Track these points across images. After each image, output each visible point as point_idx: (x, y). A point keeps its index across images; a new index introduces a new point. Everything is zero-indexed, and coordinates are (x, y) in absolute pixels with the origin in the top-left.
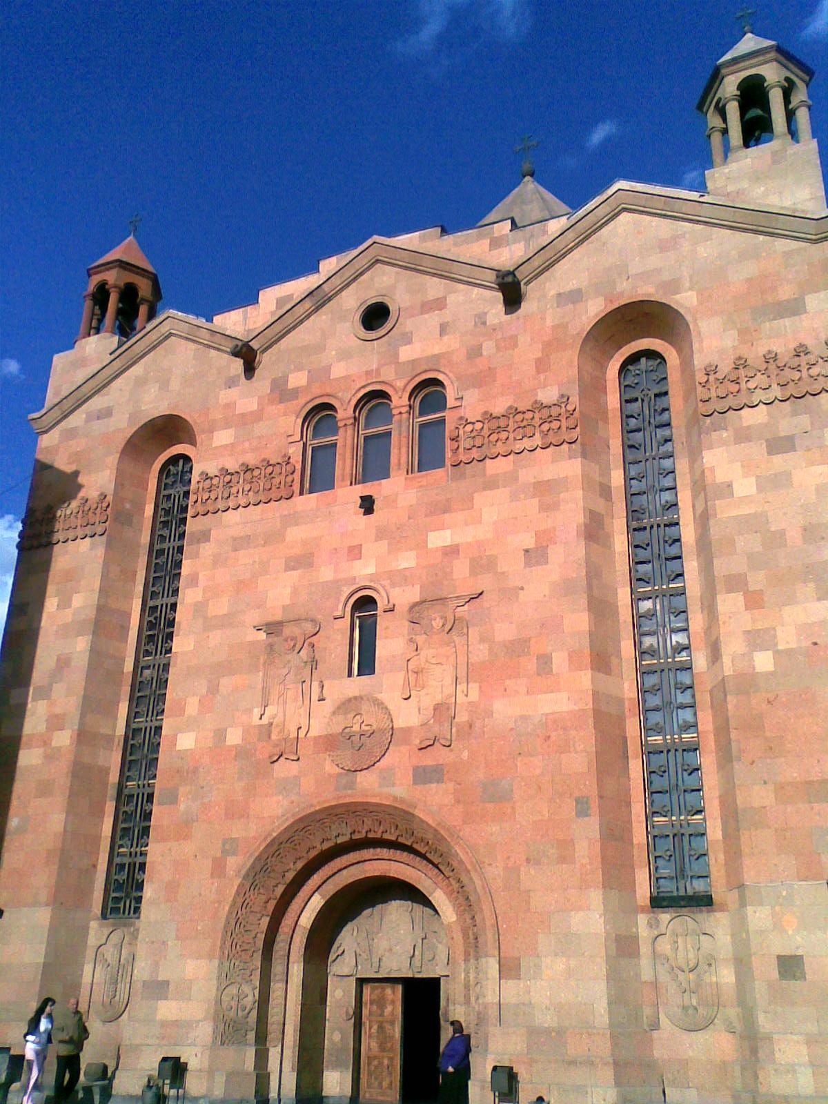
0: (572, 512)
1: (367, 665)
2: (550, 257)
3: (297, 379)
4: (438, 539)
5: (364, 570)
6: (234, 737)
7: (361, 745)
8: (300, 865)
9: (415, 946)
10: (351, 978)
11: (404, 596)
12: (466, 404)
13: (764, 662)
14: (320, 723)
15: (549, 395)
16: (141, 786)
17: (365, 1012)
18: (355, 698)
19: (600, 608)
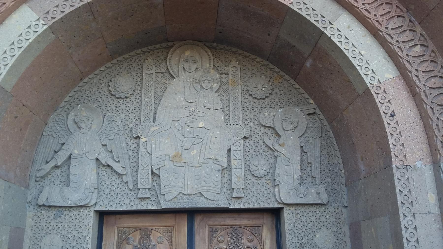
9: (229, 150)
10: (84, 212)
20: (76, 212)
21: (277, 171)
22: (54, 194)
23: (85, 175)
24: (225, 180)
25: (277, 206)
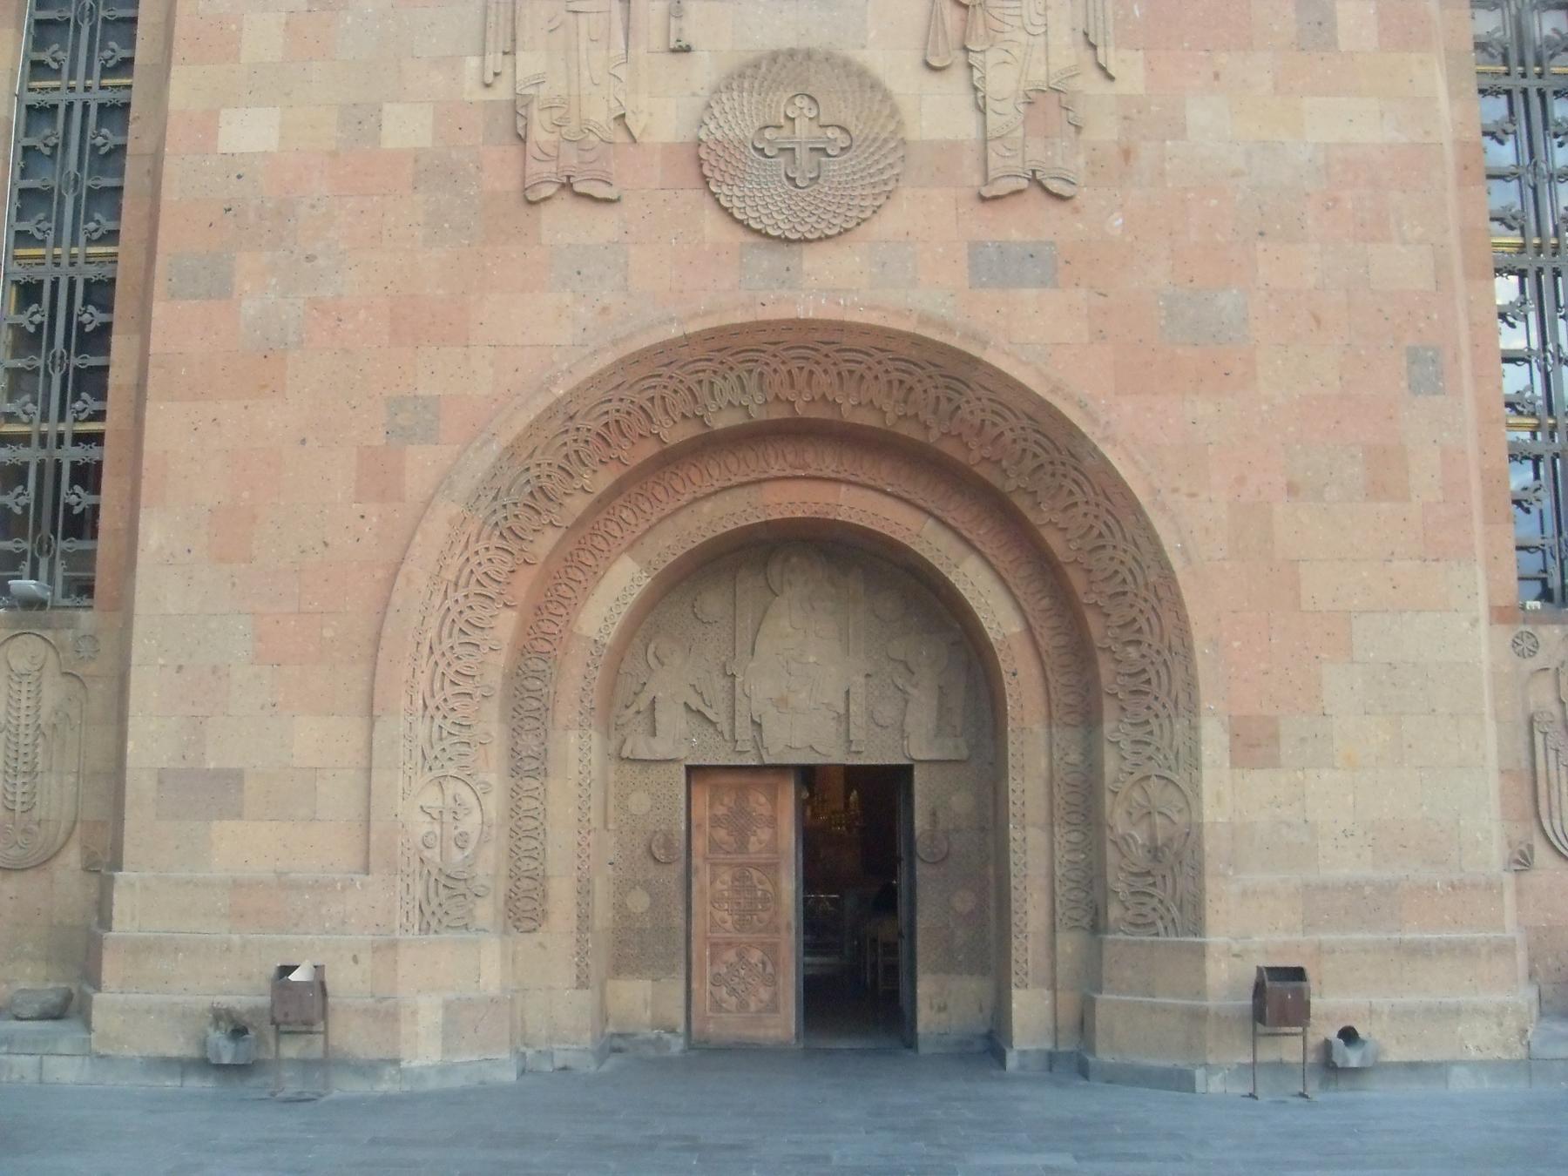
6: (407, 129)
8: (603, 480)
10: (674, 767)
16: (65, 261)
17: (699, 843)
18: (792, 54)
20: (664, 766)
21: (908, 719)
22: (640, 746)
23: (673, 721)
24: (842, 729)
25: (906, 762)
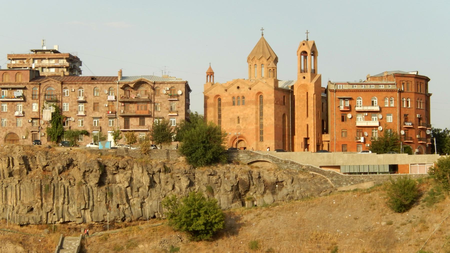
0: (254, 112)
1: (239, 123)
2: (253, 85)
3: (231, 93)
4: (244, 112)
5: (238, 114)
6: (228, 128)
7: (239, 130)
11: (242, 117)
12: (246, 99)
13: (266, 125)
14: (235, 128)
15: (253, 100)
19: (257, 119)
